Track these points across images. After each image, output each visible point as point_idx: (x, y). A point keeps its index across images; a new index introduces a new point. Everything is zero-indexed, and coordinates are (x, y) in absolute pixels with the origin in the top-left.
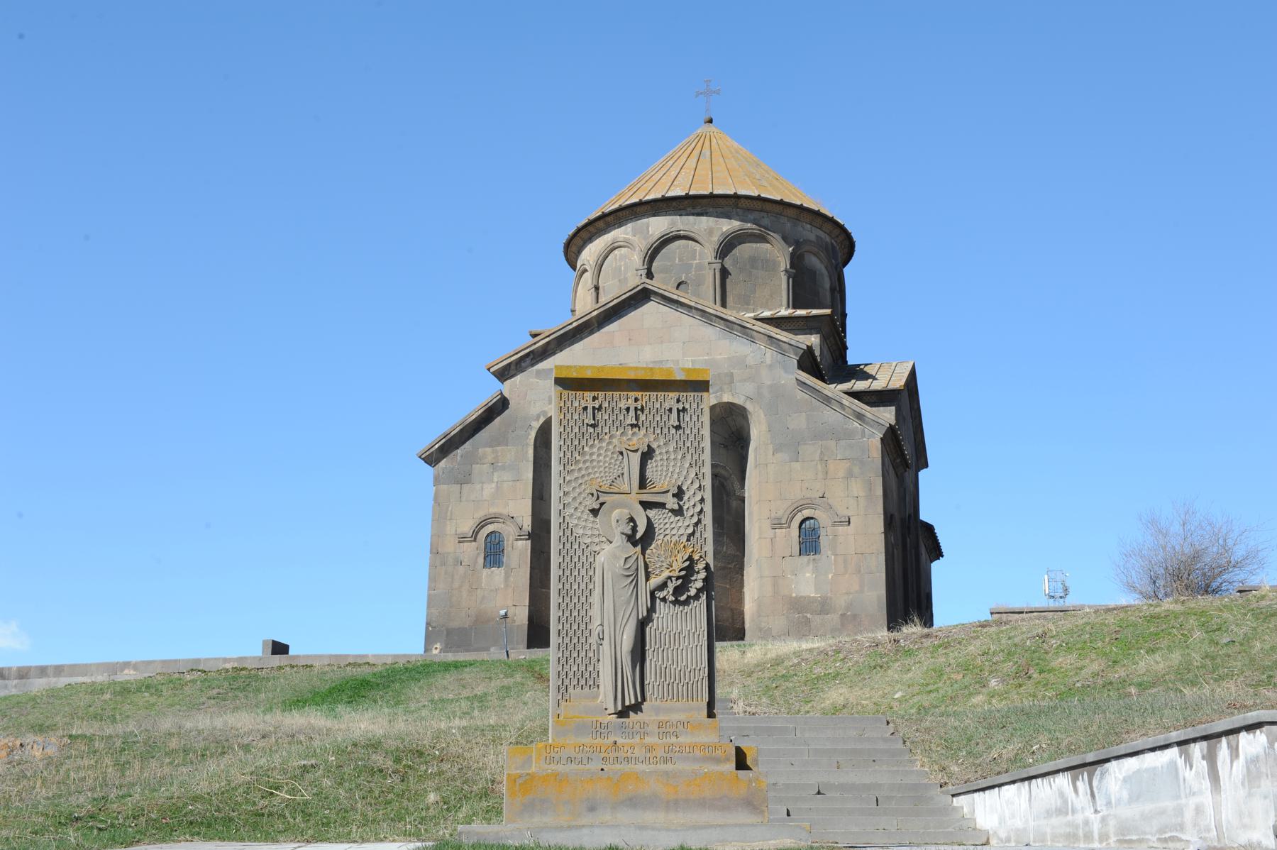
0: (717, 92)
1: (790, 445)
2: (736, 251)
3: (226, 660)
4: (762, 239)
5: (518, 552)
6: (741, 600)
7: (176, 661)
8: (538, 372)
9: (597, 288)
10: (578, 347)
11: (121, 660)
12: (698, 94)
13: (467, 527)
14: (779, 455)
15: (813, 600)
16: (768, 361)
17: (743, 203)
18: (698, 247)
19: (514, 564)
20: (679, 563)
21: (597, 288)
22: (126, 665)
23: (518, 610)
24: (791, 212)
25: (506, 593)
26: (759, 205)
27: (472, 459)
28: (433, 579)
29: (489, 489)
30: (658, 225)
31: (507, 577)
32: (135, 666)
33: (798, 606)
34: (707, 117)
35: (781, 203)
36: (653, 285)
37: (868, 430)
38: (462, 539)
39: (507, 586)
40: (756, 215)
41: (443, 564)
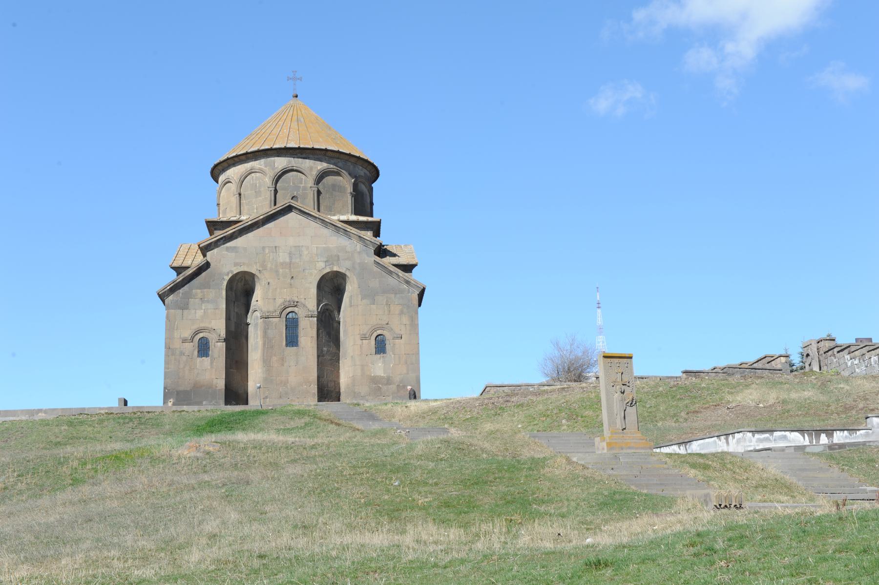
0: (300, 79)
1: (370, 295)
2: (325, 180)
3: (100, 409)
4: (338, 174)
5: (219, 349)
6: (338, 377)
7: (70, 409)
8: (227, 249)
9: (240, 194)
10: (250, 235)
11: (36, 408)
12: (289, 78)
13: (187, 334)
14: (364, 301)
15: (383, 378)
16: (358, 250)
17: (329, 154)
18: (303, 177)
19: (216, 355)
20: (631, 398)
21: (240, 194)
22: (40, 411)
23: (219, 381)
24: (353, 160)
25: (212, 371)
26: (338, 155)
27: (188, 296)
28: (167, 363)
29: (200, 313)
30: (281, 163)
31: (212, 363)
32: (46, 412)
33: (375, 380)
34: (293, 93)
35: (349, 155)
36: (294, 203)
37: (411, 289)
38: (184, 341)
39: (212, 367)
40: (335, 160)
41: (173, 354)
